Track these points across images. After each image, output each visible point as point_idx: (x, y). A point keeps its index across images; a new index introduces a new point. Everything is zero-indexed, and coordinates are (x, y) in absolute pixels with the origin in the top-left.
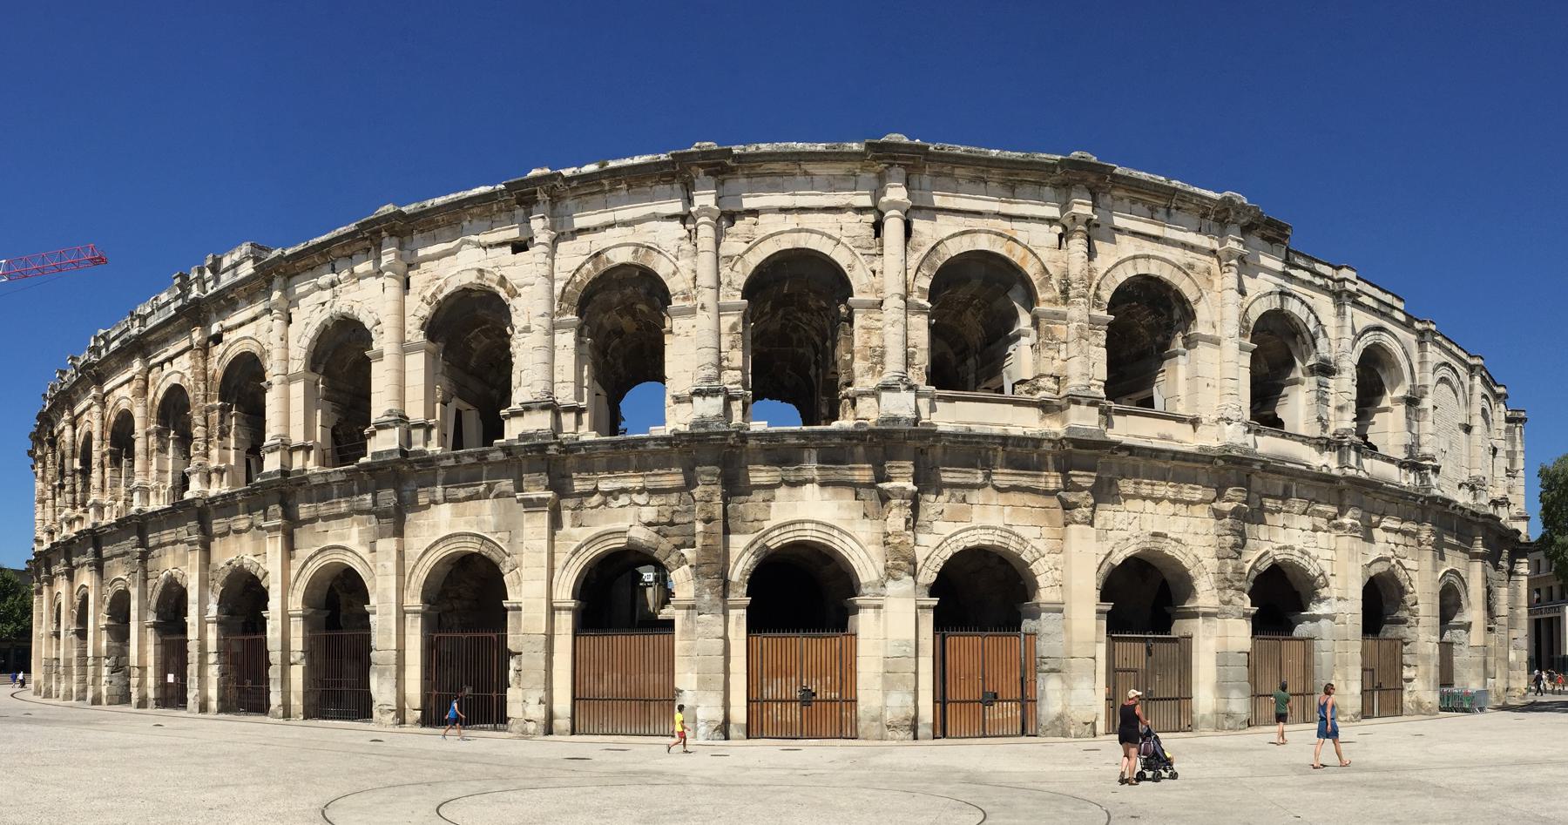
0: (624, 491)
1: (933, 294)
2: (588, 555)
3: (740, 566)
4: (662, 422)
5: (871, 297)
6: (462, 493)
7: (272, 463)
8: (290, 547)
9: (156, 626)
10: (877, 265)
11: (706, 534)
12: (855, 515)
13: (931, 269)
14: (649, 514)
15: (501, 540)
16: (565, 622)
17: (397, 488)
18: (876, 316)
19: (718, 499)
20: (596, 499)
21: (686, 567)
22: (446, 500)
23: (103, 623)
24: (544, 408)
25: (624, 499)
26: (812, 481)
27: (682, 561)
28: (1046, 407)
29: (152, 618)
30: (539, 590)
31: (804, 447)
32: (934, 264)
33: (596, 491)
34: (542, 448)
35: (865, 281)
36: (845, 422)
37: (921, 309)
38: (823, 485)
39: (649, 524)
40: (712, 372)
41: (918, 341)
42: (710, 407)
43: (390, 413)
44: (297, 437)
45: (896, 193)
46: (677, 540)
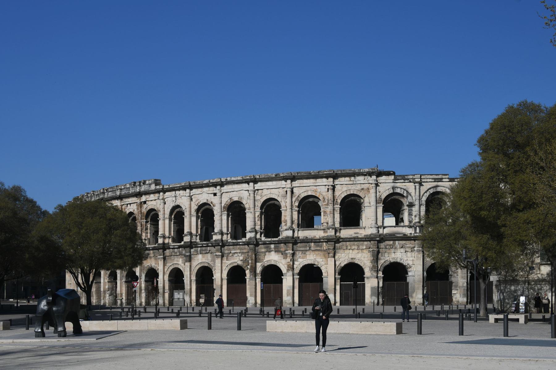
1: (299, 207)
2: (230, 267)
4: (245, 236)
5: (285, 209)
7: (160, 241)
11: (252, 263)
14: (241, 258)
16: (225, 282)
19: (254, 256)
20: (231, 254)
23: (106, 281)
25: (236, 255)
27: (248, 269)
30: (220, 276)
31: (272, 244)
36: (280, 237)
38: (275, 251)
40: (252, 227)
42: (252, 235)
43: (188, 232)
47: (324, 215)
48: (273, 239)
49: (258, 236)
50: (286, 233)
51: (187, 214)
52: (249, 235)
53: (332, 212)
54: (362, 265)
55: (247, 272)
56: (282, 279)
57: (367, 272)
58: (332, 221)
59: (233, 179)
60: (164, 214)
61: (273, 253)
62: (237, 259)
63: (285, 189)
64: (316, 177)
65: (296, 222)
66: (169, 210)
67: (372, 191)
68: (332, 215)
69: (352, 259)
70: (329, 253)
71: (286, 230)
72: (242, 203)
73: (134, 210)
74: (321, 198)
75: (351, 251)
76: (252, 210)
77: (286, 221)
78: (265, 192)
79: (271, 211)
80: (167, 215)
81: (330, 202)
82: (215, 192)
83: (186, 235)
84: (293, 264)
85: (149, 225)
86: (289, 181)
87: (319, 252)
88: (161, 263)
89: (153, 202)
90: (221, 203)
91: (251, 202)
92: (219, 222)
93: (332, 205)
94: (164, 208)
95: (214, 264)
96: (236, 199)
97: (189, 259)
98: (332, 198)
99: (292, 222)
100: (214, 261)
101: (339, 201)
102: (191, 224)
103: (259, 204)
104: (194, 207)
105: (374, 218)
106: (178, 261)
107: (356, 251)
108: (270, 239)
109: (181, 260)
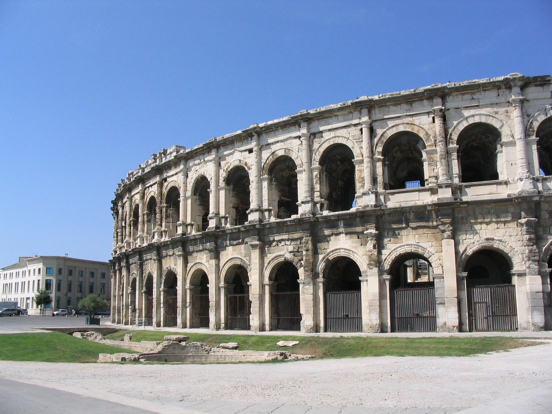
0: (283, 240)
1: (384, 153)
3: (321, 266)
5: (361, 158)
6: (235, 243)
8: (186, 262)
9: (145, 292)
11: (307, 255)
12: (358, 245)
13: (382, 143)
14: (291, 248)
15: (247, 260)
16: (267, 288)
17: (216, 241)
18: (362, 165)
20: (274, 244)
21: (302, 268)
22: (230, 245)
23: (129, 291)
24: (256, 210)
25: (283, 243)
26: (342, 233)
27: (301, 266)
28: (433, 191)
29: (144, 289)
33: (274, 241)
34: (254, 226)
36: (353, 210)
38: (346, 234)
39: (291, 252)
44: (189, 221)
46: (300, 258)
47: (429, 164)
48: (341, 212)
50: (364, 201)
51: (212, 187)
52: (304, 209)
54: (506, 250)
55: (301, 271)
56: (359, 282)
57: (519, 264)
60: (186, 190)
61: (342, 236)
62: (283, 250)
63: (359, 127)
64: (410, 100)
65: (380, 179)
66: (192, 184)
67: (515, 113)
69: (487, 239)
70: (443, 231)
71: (364, 194)
72: (291, 158)
73: (155, 193)
74: (422, 135)
75: (484, 226)
76: (305, 167)
78: (326, 136)
79: (338, 166)
80: (189, 194)
82: (249, 147)
83: (211, 218)
84: (380, 253)
85: (171, 212)
86: (365, 111)
87: (425, 230)
88: (180, 262)
89: (175, 178)
94: (185, 183)
95: (250, 260)
96: (281, 153)
97: (216, 254)
99: (374, 180)
100: (249, 255)
101: (455, 137)
102: (219, 201)
103: (317, 157)
104: (223, 174)
106: (201, 259)
107: (494, 226)
108: (337, 213)
109: (205, 256)
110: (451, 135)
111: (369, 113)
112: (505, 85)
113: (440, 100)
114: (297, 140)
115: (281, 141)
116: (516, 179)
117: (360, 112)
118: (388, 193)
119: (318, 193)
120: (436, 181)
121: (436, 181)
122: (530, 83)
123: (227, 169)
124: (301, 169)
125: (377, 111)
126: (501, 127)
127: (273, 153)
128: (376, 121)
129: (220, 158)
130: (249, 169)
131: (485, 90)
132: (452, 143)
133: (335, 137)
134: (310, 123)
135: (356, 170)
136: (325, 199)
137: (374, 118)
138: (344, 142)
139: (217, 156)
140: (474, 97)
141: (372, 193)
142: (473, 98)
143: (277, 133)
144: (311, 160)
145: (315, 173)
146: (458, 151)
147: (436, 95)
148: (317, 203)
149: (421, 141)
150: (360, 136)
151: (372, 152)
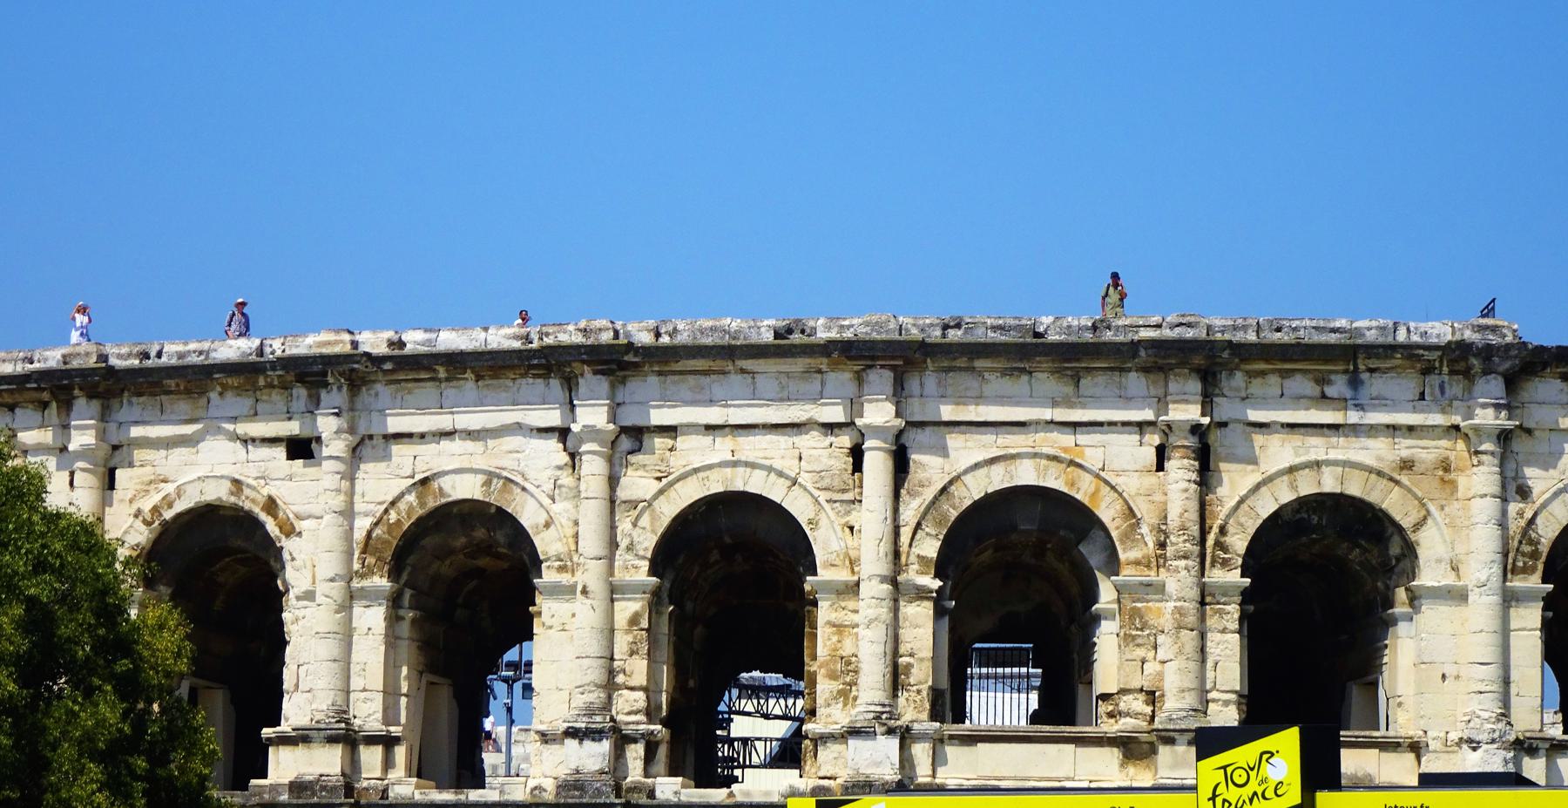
1: (941, 567)
5: (843, 575)
10: (853, 519)
13: (939, 524)
18: (851, 604)
24: (332, 740)
32: (945, 517)
35: (835, 546)
37: (921, 594)
41: (916, 645)
42: (592, 756)
45: (879, 413)
47: (1127, 640)
49: (635, 770)
53: (1191, 619)
58: (1190, 681)
59: (450, 340)
64: (1076, 361)
67: (1480, 479)
68: (1189, 638)
71: (854, 732)
74: (1108, 512)
76: (591, 575)
77: (848, 669)
81: (1178, 543)
86: (881, 378)
90: (348, 513)
91: (591, 515)
92: (330, 648)
93: (1193, 563)
98: (1193, 515)
99: (896, 679)
101: (1239, 542)
105: (1492, 672)
110: (1223, 530)
111: (899, 394)
112: (1451, 362)
113: (1195, 386)
114: (553, 445)
115: (471, 435)
116: (1454, 736)
117: (859, 379)
118: (951, 737)
119: (640, 696)
120: (1148, 710)
121: (1148, 710)
122: (1545, 365)
123: (156, 510)
124: (565, 578)
125: (931, 381)
126: (1418, 526)
127: (425, 482)
128: (922, 424)
129: (115, 448)
130: (289, 531)
131: (1371, 371)
132: (1225, 563)
133: (735, 464)
134: (623, 381)
135: (820, 622)
136: (665, 723)
137: (917, 412)
138: (775, 491)
139: (102, 435)
140: (1331, 391)
141: (890, 731)
142: (1324, 396)
143: (450, 392)
144: (613, 544)
145: (627, 608)
146: (1247, 596)
147: (1182, 364)
148: (633, 740)
149: (1097, 534)
150: (847, 476)
151: (897, 554)
